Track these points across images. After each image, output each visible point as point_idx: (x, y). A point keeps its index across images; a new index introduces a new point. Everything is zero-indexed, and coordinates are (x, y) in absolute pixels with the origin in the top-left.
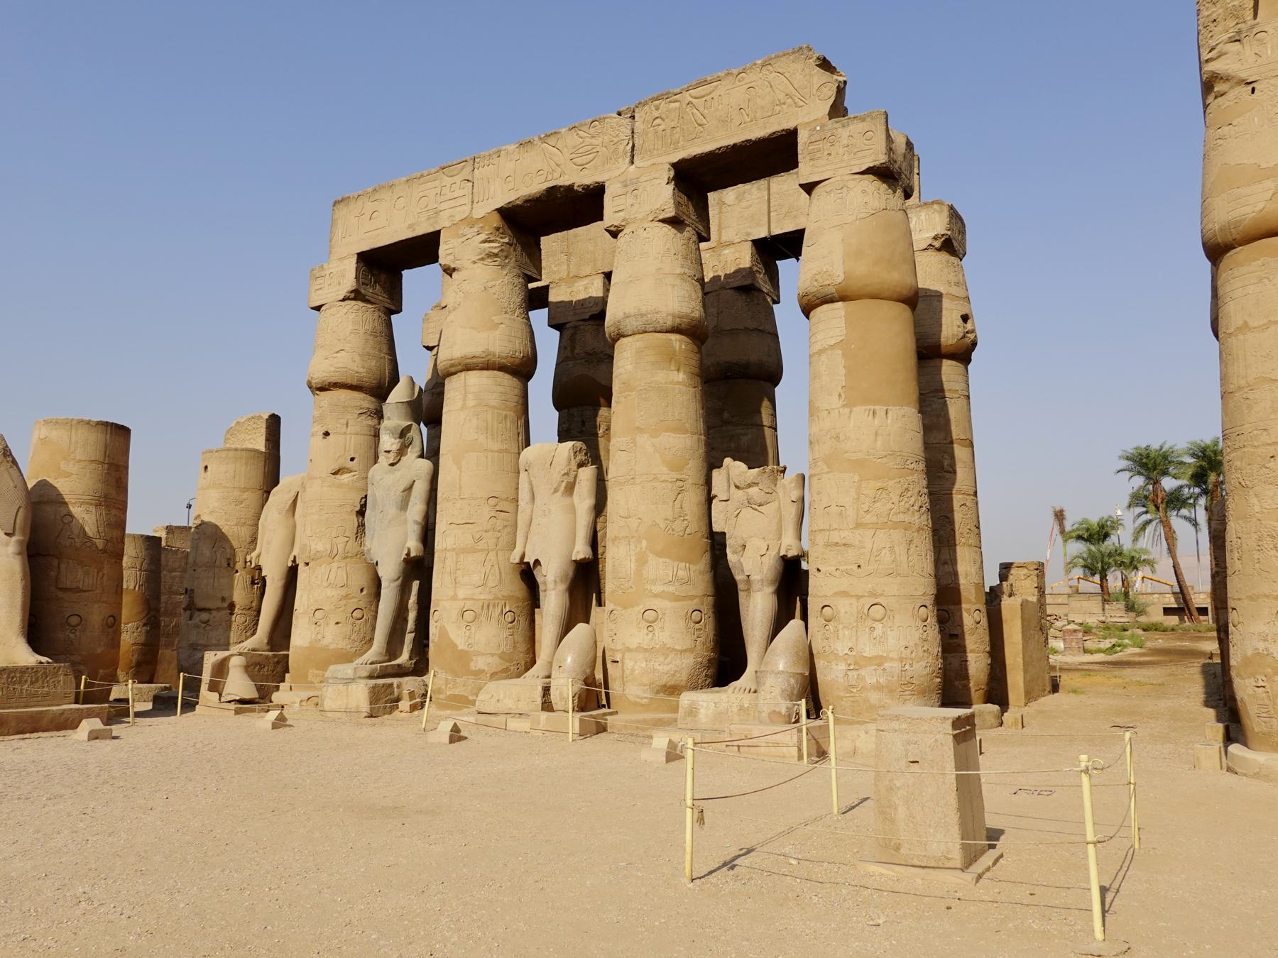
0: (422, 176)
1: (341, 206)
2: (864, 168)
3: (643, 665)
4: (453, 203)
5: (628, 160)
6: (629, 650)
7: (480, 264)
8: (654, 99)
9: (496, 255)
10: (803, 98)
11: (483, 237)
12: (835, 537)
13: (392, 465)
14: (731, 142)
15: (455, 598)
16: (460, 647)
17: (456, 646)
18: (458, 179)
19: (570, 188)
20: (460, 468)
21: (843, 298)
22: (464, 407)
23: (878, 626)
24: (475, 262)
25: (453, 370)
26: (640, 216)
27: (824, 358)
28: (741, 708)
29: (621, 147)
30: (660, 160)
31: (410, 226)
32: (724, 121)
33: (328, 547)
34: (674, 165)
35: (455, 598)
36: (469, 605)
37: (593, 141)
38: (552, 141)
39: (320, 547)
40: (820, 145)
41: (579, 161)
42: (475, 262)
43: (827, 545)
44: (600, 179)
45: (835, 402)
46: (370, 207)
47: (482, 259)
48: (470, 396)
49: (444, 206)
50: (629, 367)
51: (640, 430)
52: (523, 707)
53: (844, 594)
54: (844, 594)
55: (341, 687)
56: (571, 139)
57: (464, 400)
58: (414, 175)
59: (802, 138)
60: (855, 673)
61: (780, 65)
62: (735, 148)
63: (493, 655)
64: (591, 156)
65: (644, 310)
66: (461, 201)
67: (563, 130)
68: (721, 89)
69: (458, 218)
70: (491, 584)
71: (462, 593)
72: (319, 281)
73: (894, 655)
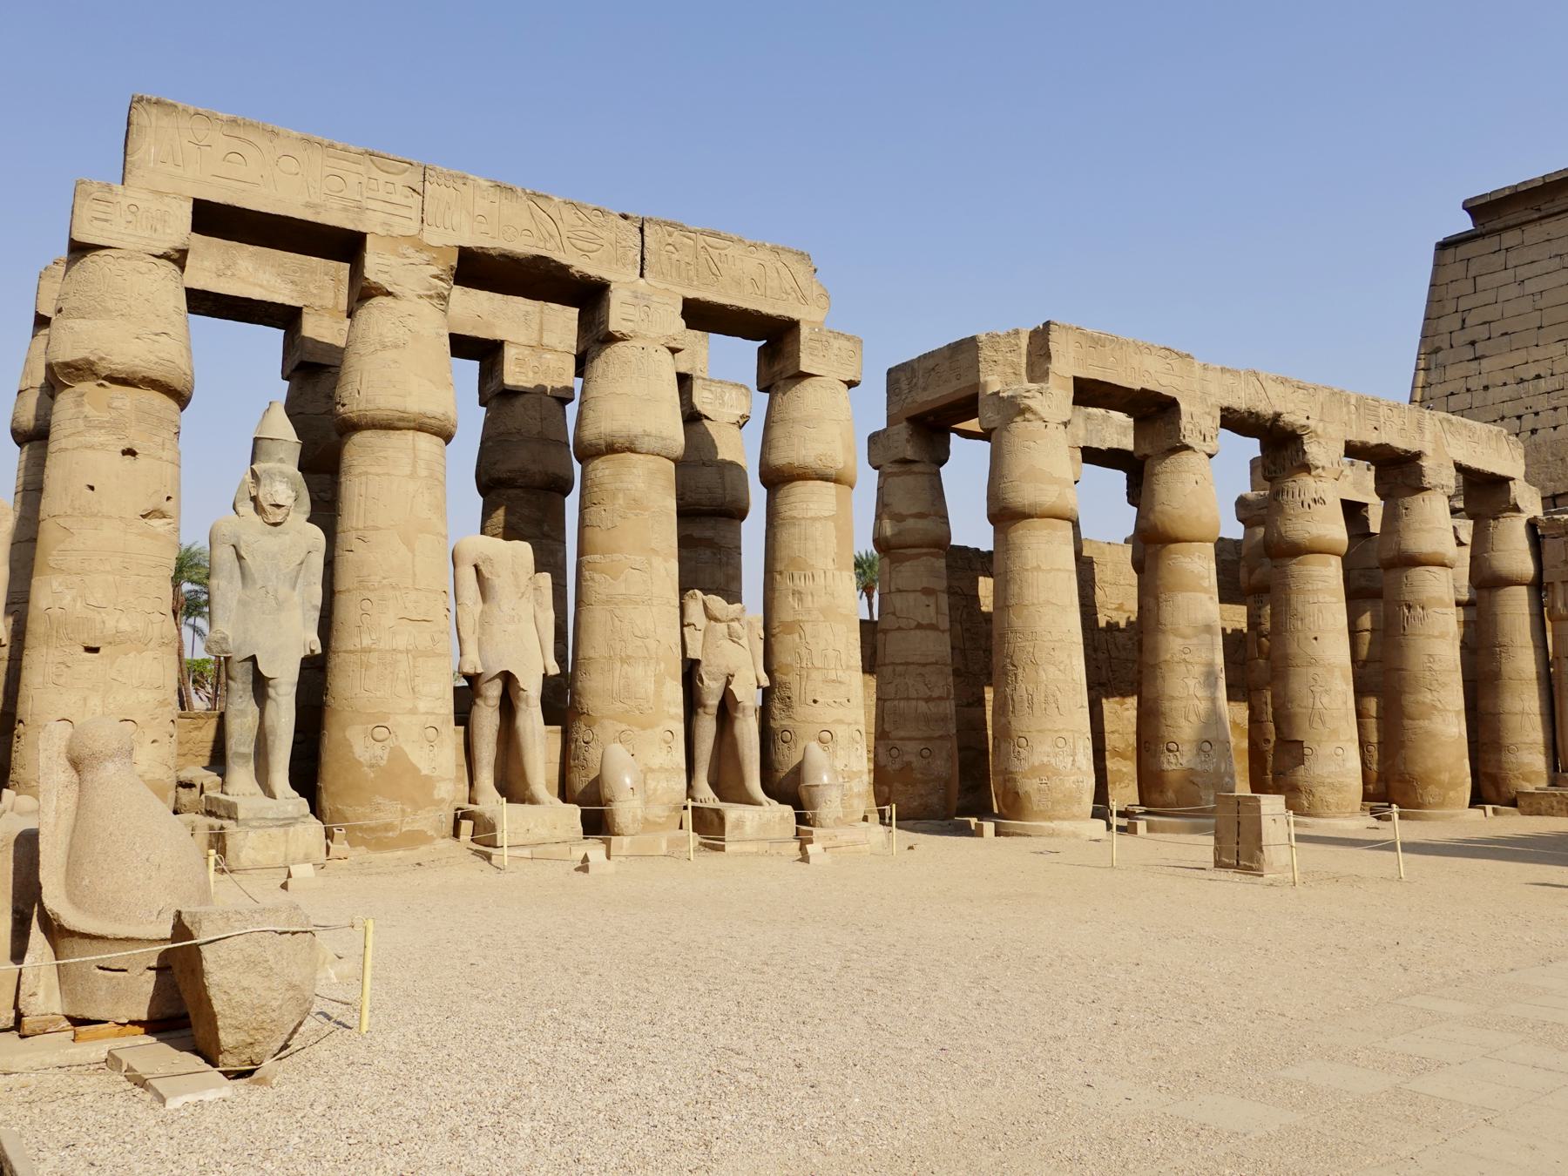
0: (332, 146)
1: (154, 110)
4: (389, 208)
6: (652, 770)
7: (425, 301)
8: (666, 224)
10: (804, 297)
11: (435, 270)
12: (832, 675)
13: (275, 524)
14: (745, 305)
15: (413, 711)
16: (424, 772)
17: (416, 770)
18: (399, 180)
19: (565, 268)
20: (412, 551)
21: (836, 481)
22: (413, 475)
24: (420, 297)
25: (401, 424)
27: (818, 525)
28: (782, 818)
29: (631, 254)
30: (673, 288)
31: (308, 205)
32: (738, 283)
34: (686, 302)
35: (413, 711)
36: (431, 721)
38: (540, 202)
39: (125, 625)
40: (818, 345)
41: (579, 244)
42: (420, 297)
43: (826, 681)
44: (606, 276)
45: (831, 566)
46: (220, 142)
47: (430, 297)
48: (421, 463)
50: (641, 485)
51: (655, 552)
52: (560, 834)
53: (840, 722)
54: (840, 722)
55: (274, 831)
56: (569, 215)
57: (414, 466)
58: (318, 138)
59: (804, 331)
61: (788, 258)
62: (723, 307)
64: (595, 247)
65: (664, 434)
66: (405, 212)
67: (556, 199)
68: (733, 250)
69: (397, 231)
71: (422, 706)
72: (101, 207)
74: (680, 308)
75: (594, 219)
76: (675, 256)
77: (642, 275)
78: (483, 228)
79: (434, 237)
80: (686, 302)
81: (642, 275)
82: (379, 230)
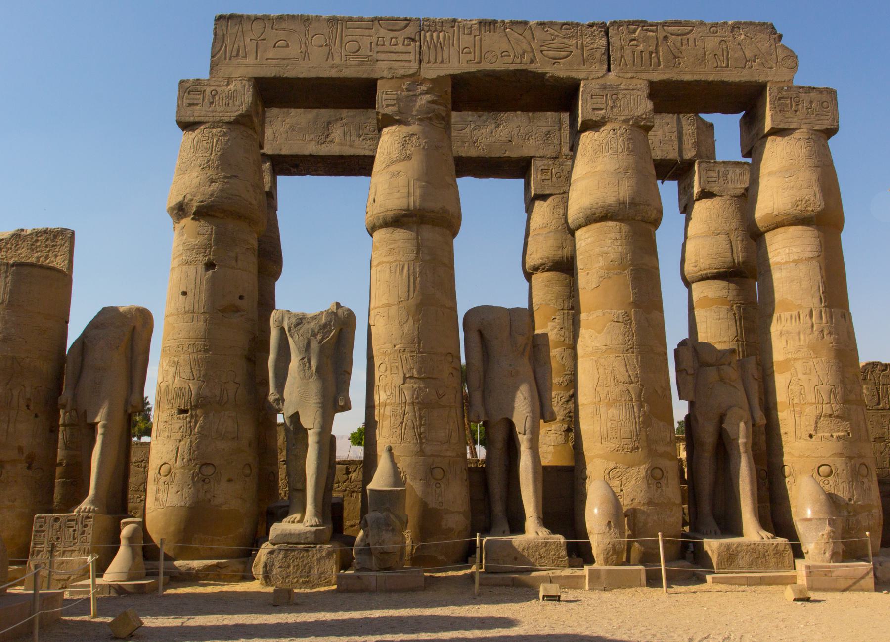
2: (825, 127)
3: (655, 518)
4: (394, 57)
5: (605, 67)
9: (443, 118)
23: (865, 480)
26: (623, 118)
29: (598, 55)
31: (332, 67)
33: (217, 392)
34: (652, 84)
37: (566, 40)
38: (514, 27)
41: (551, 54)
44: (574, 74)
49: (381, 56)
60: (854, 519)
63: (459, 513)
69: (401, 72)
70: (453, 441)
73: (875, 504)
74: (646, 93)
75: (564, 32)
76: (641, 47)
77: (609, 70)
78: (469, 57)
79: (431, 71)
80: (652, 84)
81: (609, 70)
82: (385, 74)
